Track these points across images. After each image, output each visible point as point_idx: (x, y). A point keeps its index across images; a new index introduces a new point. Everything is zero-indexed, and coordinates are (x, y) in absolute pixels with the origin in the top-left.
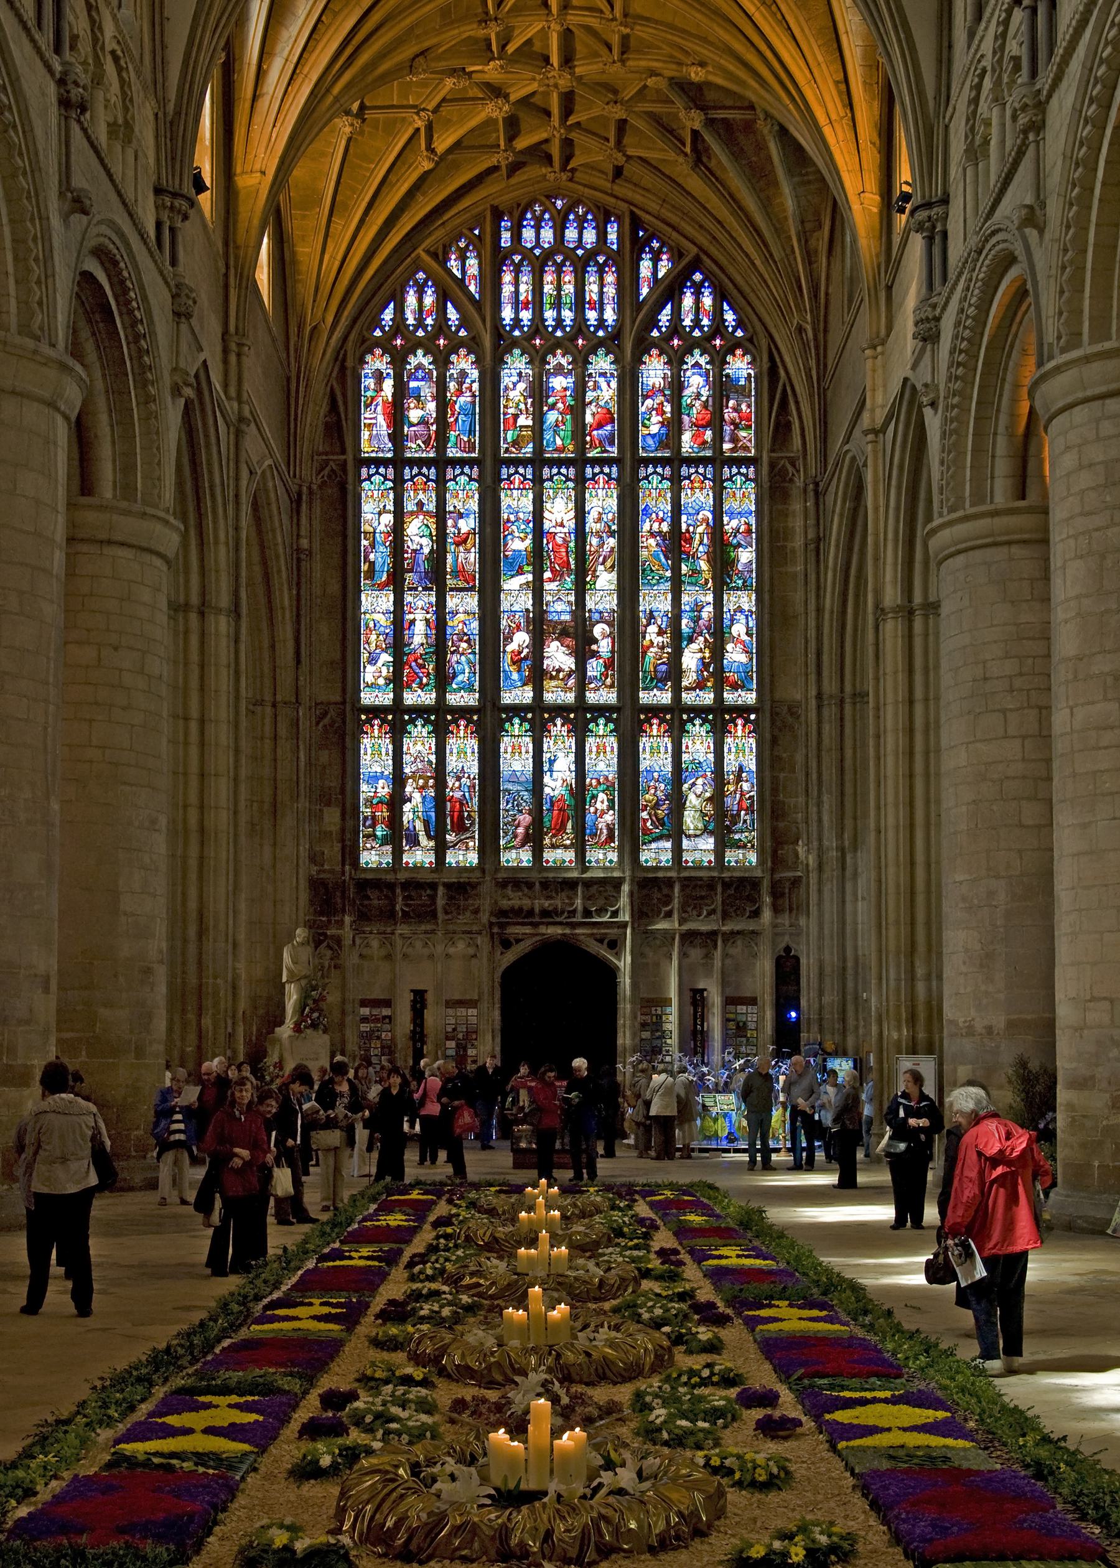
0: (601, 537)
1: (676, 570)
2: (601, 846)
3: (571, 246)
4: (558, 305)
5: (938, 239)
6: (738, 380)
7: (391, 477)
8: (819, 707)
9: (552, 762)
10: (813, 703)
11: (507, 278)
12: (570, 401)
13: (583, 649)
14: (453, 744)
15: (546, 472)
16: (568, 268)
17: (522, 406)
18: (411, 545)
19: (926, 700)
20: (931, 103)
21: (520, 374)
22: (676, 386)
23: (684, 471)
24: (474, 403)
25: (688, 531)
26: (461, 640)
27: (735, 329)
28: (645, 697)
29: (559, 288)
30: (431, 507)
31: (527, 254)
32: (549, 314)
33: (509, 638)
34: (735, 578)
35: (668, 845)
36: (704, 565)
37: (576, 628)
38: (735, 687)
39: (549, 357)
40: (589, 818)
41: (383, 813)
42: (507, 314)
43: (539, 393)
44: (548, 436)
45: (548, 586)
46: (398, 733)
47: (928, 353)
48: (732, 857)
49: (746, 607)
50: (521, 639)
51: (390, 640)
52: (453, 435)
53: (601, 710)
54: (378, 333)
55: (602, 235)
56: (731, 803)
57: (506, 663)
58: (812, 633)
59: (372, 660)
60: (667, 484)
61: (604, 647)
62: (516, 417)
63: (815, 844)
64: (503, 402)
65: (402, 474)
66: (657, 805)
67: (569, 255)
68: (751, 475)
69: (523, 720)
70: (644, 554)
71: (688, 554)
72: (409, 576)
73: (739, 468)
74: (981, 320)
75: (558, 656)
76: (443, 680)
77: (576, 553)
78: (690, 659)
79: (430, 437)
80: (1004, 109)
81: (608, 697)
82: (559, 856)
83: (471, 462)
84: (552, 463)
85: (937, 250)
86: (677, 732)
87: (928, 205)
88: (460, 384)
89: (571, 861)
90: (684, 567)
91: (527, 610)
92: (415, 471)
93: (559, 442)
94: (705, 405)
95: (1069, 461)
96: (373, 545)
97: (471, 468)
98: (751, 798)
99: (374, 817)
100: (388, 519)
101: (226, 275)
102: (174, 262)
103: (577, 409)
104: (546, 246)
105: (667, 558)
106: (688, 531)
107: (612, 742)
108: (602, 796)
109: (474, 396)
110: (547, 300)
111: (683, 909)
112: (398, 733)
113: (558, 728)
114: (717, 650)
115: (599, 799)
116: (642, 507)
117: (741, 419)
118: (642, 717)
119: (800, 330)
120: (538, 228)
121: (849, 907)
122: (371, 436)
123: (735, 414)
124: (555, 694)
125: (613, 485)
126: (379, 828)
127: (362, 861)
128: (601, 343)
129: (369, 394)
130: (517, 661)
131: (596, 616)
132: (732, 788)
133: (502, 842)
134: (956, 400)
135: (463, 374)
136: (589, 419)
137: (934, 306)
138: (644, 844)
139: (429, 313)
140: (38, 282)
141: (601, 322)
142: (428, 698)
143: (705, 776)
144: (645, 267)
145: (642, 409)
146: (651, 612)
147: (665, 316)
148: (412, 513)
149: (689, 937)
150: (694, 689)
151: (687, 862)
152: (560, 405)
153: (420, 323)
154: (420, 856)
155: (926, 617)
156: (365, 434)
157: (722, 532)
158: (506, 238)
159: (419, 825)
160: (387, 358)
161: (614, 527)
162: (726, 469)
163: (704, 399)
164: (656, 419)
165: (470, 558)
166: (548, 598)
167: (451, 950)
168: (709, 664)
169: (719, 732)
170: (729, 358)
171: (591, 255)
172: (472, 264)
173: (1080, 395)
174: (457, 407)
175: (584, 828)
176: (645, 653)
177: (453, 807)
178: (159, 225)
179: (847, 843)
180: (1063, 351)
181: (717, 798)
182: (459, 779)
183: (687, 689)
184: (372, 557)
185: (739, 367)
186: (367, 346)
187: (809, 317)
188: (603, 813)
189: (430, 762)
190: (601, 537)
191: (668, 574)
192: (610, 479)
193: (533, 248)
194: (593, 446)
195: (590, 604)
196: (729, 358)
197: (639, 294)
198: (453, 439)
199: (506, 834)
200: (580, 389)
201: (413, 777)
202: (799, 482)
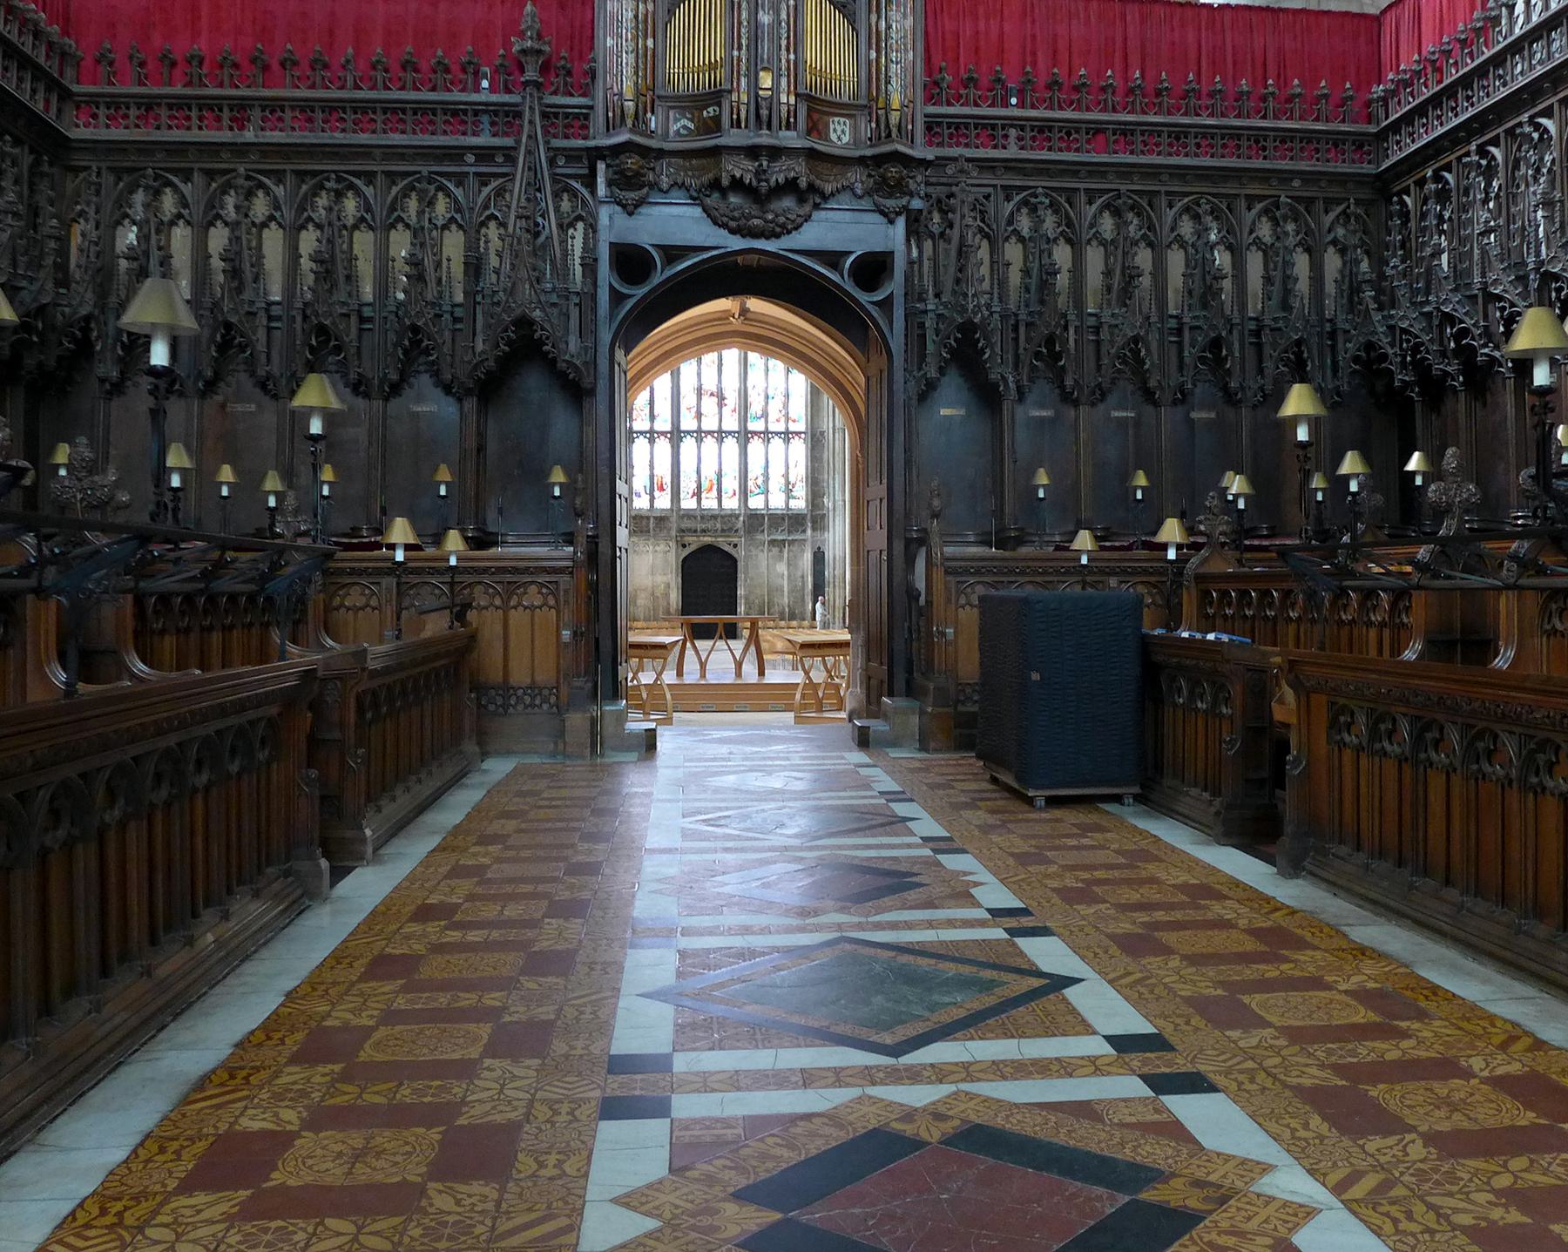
28: (752, 426)
35: (762, 497)
48: (793, 504)
56: (792, 479)
76: (652, 417)
78: (775, 408)
82: (709, 503)
111: (770, 527)
114: (786, 405)
124: (710, 423)
149: (772, 543)
167: (657, 548)
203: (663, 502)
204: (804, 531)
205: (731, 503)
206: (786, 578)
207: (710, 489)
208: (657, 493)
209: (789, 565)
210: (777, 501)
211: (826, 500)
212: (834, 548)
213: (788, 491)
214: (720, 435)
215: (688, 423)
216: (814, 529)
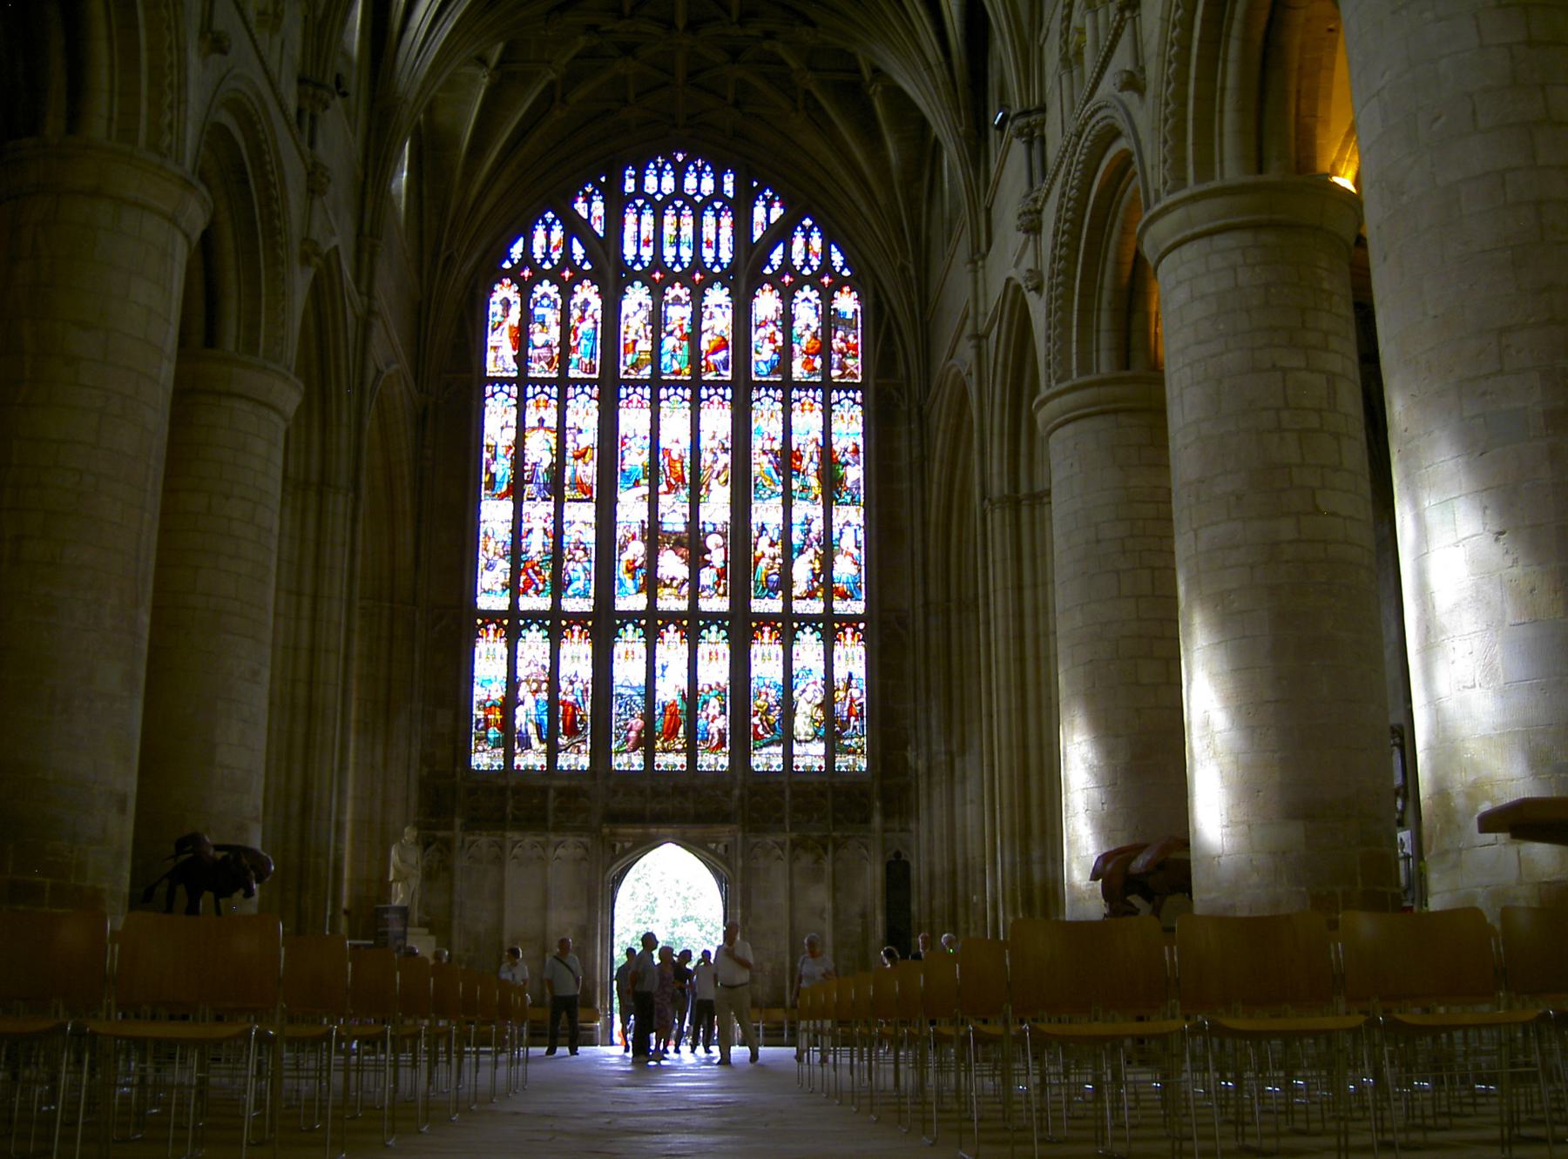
0: (715, 454)
1: (787, 485)
2: (713, 750)
3: (691, 193)
4: (677, 243)
5: (1036, 144)
6: (845, 314)
7: (515, 395)
8: (926, 616)
9: (664, 668)
10: (920, 611)
11: (630, 218)
12: (687, 329)
13: (696, 557)
14: (566, 649)
15: (663, 393)
16: (687, 211)
17: (641, 333)
18: (530, 458)
19: (1035, 586)
20: (1026, 30)
21: (640, 305)
22: (787, 319)
23: (795, 394)
24: (595, 329)
25: (798, 450)
26: (578, 548)
27: (842, 269)
28: (757, 606)
29: (678, 229)
30: (552, 421)
31: (649, 199)
32: (669, 253)
33: (624, 547)
34: (844, 494)
35: (779, 750)
36: (813, 481)
37: (690, 538)
38: (844, 596)
39: (668, 290)
40: (701, 723)
41: (497, 716)
42: (629, 251)
43: (657, 321)
44: (666, 359)
45: (662, 498)
46: (512, 638)
47: (1031, 245)
48: (842, 762)
49: (854, 522)
50: (637, 550)
51: (508, 548)
52: (574, 357)
53: (713, 618)
54: (507, 265)
55: (719, 184)
56: (841, 709)
57: (621, 571)
58: (918, 546)
59: (490, 566)
60: (779, 406)
61: (717, 557)
62: (635, 342)
63: (923, 749)
64: (623, 328)
65: (526, 393)
66: (768, 711)
67: (688, 200)
68: (858, 400)
69: (637, 626)
70: (755, 470)
71: (798, 471)
72: (528, 488)
73: (847, 392)
74: (1085, 187)
75: (672, 565)
76: (559, 586)
77: (691, 468)
78: (802, 570)
79: (553, 359)
80: (1096, 15)
81: (719, 604)
82: (671, 760)
83: (591, 383)
84: (668, 384)
85: (1036, 154)
86: (788, 640)
87: (1026, 113)
88: (584, 312)
89: (682, 766)
90: (794, 481)
91: (643, 522)
92: (538, 389)
93: (676, 367)
94: (814, 336)
95: (1181, 295)
96: (494, 458)
97: (592, 388)
98: (861, 704)
99: (486, 720)
100: (511, 434)
101: (364, 183)
102: (312, 144)
103: (694, 337)
104: (667, 192)
105: (778, 474)
106: (798, 450)
107: (724, 648)
108: (714, 702)
109: (596, 322)
110: (667, 239)
112: (512, 638)
113: (672, 635)
114: (827, 562)
115: (711, 704)
116: (754, 426)
117: (849, 349)
118: (754, 624)
119: (903, 269)
120: (659, 177)
121: (958, 811)
122: (496, 358)
123: (843, 345)
124: (670, 602)
125: (727, 404)
126: (491, 730)
127: (474, 763)
128: (717, 278)
129: (498, 318)
130: (632, 569)
131: (709, 528)
132: (841, 694)
133: (614, 746)
134: (1061, 278)
135: (586, 303)
136: (705, 346)
137: (1035, 200)
138: (755, 749)
139: (556, 248)
140: (171, 107)
141: (717, 260)
142: (543, 603)
143: (815, 683)
144: (759, 213)
145: (755, 338)
146: (763, 525)
147: (777, 257)
148: (534, 429)
150: (804, 598)
151: (797, 767)
152: (678, 333)
153: (547, 256)
154: (532, 759)
155: (1032, 508)
156: (490, 355)
157: (832, 452)
158: (630, 186)
159: (532, 729)
160: (515, 287)
161: (728, 445)
162: (834, 393)
163: (813, 329)
164: (769, 346)
165: (588, 471)
166: (661, 510)
168: (819, 575)
169: (829, 640)
170: (837, 294)
171: (709, 201)
172: (598, 207)
173: (1189, 232)
174: (579, 333)
175: (697, 734)
176: (756, 563)
177: (565, 711)
178: (300, 112)
179: (955, 748)
180: (1169, 193)
181: (828, 704)
182: (572, 683)
183: (797, 598)
184: (493, 469)
185: (846, 303)
186: (499, 276)
187: (911, 258)
188: (714, 718)
189: (544, 667)
190: (715, 454)
191: (780, 489)
192: (724, 400)
193: (655, 194)
194: (708, 370)
195: (703, 516)
196: (837, 294)
197: (752, 236)
198: (574, 362)
199: (618, 738)
200: (697, 318)
201: (527, 681)
202: (904, 408)
203: (576, 759)
204: (867, 820)
205: (714, 761)
206: (828, 916)
207: (671, 733)
208: (563, 741)
209: (835, 889)
210: (811, 755)
211: (910, 755)
212: (930, 852)
213: (831, 731)
214: (692, 624)
215: (630, 599)
216: (887, 815)
